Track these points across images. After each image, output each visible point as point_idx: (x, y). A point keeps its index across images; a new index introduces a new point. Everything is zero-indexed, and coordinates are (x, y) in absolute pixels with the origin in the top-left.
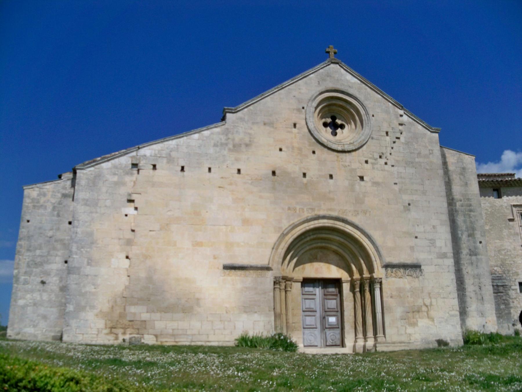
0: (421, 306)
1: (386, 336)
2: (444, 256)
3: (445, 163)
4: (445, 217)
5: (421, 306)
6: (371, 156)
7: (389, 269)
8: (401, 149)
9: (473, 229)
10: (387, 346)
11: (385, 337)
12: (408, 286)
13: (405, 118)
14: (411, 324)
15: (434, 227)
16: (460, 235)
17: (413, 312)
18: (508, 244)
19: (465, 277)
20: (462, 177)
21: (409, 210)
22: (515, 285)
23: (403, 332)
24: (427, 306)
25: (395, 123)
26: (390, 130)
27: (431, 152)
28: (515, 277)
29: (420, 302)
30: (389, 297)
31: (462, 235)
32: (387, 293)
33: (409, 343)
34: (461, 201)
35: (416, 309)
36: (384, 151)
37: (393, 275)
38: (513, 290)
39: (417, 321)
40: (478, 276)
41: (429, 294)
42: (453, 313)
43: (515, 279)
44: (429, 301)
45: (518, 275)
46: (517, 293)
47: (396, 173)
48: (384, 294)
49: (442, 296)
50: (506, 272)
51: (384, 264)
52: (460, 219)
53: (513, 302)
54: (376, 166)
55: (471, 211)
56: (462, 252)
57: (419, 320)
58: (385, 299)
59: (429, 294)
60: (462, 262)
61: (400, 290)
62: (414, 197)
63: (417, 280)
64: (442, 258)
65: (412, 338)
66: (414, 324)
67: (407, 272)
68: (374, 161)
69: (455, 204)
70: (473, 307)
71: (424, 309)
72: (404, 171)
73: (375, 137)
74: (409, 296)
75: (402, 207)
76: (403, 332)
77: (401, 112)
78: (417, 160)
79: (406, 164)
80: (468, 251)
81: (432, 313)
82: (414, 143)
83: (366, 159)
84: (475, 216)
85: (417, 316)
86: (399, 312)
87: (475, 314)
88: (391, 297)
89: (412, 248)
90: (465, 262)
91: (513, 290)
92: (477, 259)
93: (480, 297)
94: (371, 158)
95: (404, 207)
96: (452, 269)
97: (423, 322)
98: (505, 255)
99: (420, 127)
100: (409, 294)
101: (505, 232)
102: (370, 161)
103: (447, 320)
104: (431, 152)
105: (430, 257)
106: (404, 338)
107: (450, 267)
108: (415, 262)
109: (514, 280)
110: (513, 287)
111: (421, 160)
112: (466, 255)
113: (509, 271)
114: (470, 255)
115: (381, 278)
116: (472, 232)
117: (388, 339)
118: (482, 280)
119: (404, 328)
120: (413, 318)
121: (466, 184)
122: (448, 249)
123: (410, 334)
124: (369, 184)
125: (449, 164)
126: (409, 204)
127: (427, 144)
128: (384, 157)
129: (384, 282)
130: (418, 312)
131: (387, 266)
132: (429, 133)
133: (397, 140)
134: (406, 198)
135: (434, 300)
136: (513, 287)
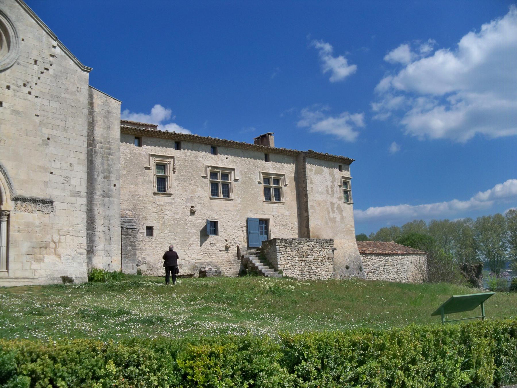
0: (50, 242)
1: (10, 271)
2: (77, 194)
3: (91, 104)
4: (84, 157)
6: (14, 82)
7: (19, 202)
8: (48, 82)
9: (110, 172)
10: (9, 281)
11: (8, 272)
12: (37, 222)
13: (58, 50)
14: (37, 260)
15: (71, 165)
16: (96, 176)
17: (41, 248)
18: (142, 190)
19: (96, 217)
20: (106, 120)
21: (48, 145)
22: (143, 229)
23: (28, 268)
24: (55, 243)
25: (47, 53)
26: (39, 59)
27: (79, 90)
28: (144, 222)
29: (48, 238)
30: (16, 231)
31: (98, 176)
32: (14, 227)
33: (33, 278)
34: (101, 143)
35: (43, 245)
36: (30, 80)
37: (24, 209)
38: (141, 233)
39: (44, 257)
40: (108, 218)
41: (59, 231)
42: (80, 251)
43: (144, 224)
44: (58, 238)
45: (147, 220)
46: (143, 236)
47: (39, 104)
48: (11, 228)
49: (71, 234)
50: (136, 216)
51: (15, 196)
52: (98, 161)
53: (140, 245)
54: (18, 94)
55: (109, 154)
56: (96, 193)
57: (46, 256)
58: (11, 233)
59: (59, 231)
60: (94, 203)
61: (28, 225)
62: (55, 133)
63: (47, 215)
65: (36, 275)
66: (40, 260)
67: (38, 206)
68: (16, 88)
69: (96, 145)
70: (100, 246)
71: (52, 245)
72: (48, 104)
73: (21, 62)
74: (38, 231)
75: (41, 141)
76: (28, 268)
77: (55, 43)
78: (63, 95)
79: (52, 97)
80: (102, 192)
81: (60, 250)
82: (63, 78)
83: (8, 84)
84: (112, 159)
85: (44, 252)
86: (25, 246)
87: (102, 253)
88: (18, 231)
89: (46, 183)
90: (98, 203)
91: (141, 233)
92: (110, 200)
93: (108, 238)
94: (13, 84)
95: (43, 140)
96: (84, 208)
97: (49, 259)
98: (138, 200)
99: (71, 62)
101: (141, 179)
102: (12, 87)
103: (73, 257)
104: (79, 89)
105: (64, 194)
106: (28, 274)
107: (82, 206)
108: (47, 197)
109: (142, 224)
110: (141, 231)
111: (67, 96)
112: (100, 196)
113: (139, 215)
114: (104, 196)
115: (9, 211)
116: (108, 175)
117: (11, 274)
118: (112, 221)
119: (29, 263)
120: (40, 254)
121: (109, 127)
122: (83, 188)
123: (35, 270)
124: (8, 111)
125: (95, 105)
126: (48, 139)
127: (76, 82)
128: (28, 85)
129: (12, 214)
130: (46, 248)
131: (17, 199)
132: (80, 70)
133: (45, 71)
134: (46, 132)
135: (62, 237)
136: (141, 231)
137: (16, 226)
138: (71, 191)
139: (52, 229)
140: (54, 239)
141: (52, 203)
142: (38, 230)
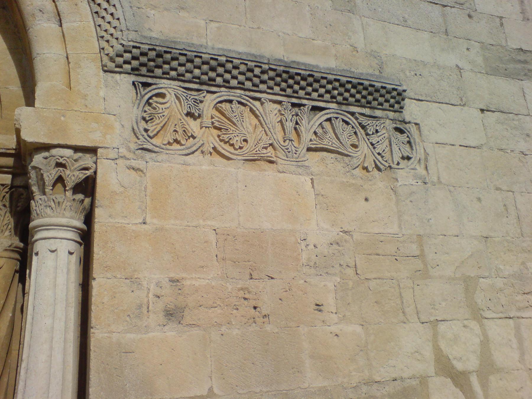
0: (423, 380)
5: (423, 380)
12: (318, 230)
30: (155, 318)
32: (133, 280)
41: (469, 284)
51: (128, 38)
58: (97, 335)
59: (469, 284)
63: (379, 182)
64: (508, 75)
67: (311, 124)
74: (330, 302)
88: (173, 314)
100: (326, 288)
105: (451, 59)
108: (363, 68)
129: (111, 178)
131: (148, 64)
137: (154, 277)
138: (483, 46)
139: (424, 274)
140: (452, 352)
141: (392, 98)
142: (326, 288)
